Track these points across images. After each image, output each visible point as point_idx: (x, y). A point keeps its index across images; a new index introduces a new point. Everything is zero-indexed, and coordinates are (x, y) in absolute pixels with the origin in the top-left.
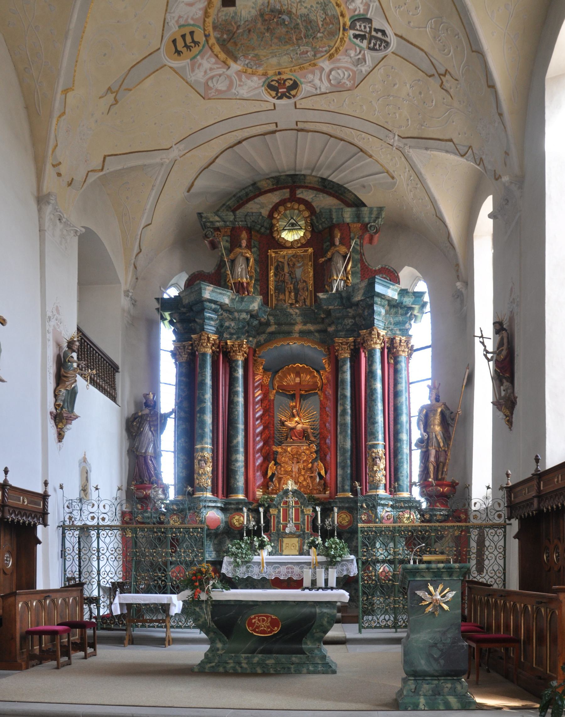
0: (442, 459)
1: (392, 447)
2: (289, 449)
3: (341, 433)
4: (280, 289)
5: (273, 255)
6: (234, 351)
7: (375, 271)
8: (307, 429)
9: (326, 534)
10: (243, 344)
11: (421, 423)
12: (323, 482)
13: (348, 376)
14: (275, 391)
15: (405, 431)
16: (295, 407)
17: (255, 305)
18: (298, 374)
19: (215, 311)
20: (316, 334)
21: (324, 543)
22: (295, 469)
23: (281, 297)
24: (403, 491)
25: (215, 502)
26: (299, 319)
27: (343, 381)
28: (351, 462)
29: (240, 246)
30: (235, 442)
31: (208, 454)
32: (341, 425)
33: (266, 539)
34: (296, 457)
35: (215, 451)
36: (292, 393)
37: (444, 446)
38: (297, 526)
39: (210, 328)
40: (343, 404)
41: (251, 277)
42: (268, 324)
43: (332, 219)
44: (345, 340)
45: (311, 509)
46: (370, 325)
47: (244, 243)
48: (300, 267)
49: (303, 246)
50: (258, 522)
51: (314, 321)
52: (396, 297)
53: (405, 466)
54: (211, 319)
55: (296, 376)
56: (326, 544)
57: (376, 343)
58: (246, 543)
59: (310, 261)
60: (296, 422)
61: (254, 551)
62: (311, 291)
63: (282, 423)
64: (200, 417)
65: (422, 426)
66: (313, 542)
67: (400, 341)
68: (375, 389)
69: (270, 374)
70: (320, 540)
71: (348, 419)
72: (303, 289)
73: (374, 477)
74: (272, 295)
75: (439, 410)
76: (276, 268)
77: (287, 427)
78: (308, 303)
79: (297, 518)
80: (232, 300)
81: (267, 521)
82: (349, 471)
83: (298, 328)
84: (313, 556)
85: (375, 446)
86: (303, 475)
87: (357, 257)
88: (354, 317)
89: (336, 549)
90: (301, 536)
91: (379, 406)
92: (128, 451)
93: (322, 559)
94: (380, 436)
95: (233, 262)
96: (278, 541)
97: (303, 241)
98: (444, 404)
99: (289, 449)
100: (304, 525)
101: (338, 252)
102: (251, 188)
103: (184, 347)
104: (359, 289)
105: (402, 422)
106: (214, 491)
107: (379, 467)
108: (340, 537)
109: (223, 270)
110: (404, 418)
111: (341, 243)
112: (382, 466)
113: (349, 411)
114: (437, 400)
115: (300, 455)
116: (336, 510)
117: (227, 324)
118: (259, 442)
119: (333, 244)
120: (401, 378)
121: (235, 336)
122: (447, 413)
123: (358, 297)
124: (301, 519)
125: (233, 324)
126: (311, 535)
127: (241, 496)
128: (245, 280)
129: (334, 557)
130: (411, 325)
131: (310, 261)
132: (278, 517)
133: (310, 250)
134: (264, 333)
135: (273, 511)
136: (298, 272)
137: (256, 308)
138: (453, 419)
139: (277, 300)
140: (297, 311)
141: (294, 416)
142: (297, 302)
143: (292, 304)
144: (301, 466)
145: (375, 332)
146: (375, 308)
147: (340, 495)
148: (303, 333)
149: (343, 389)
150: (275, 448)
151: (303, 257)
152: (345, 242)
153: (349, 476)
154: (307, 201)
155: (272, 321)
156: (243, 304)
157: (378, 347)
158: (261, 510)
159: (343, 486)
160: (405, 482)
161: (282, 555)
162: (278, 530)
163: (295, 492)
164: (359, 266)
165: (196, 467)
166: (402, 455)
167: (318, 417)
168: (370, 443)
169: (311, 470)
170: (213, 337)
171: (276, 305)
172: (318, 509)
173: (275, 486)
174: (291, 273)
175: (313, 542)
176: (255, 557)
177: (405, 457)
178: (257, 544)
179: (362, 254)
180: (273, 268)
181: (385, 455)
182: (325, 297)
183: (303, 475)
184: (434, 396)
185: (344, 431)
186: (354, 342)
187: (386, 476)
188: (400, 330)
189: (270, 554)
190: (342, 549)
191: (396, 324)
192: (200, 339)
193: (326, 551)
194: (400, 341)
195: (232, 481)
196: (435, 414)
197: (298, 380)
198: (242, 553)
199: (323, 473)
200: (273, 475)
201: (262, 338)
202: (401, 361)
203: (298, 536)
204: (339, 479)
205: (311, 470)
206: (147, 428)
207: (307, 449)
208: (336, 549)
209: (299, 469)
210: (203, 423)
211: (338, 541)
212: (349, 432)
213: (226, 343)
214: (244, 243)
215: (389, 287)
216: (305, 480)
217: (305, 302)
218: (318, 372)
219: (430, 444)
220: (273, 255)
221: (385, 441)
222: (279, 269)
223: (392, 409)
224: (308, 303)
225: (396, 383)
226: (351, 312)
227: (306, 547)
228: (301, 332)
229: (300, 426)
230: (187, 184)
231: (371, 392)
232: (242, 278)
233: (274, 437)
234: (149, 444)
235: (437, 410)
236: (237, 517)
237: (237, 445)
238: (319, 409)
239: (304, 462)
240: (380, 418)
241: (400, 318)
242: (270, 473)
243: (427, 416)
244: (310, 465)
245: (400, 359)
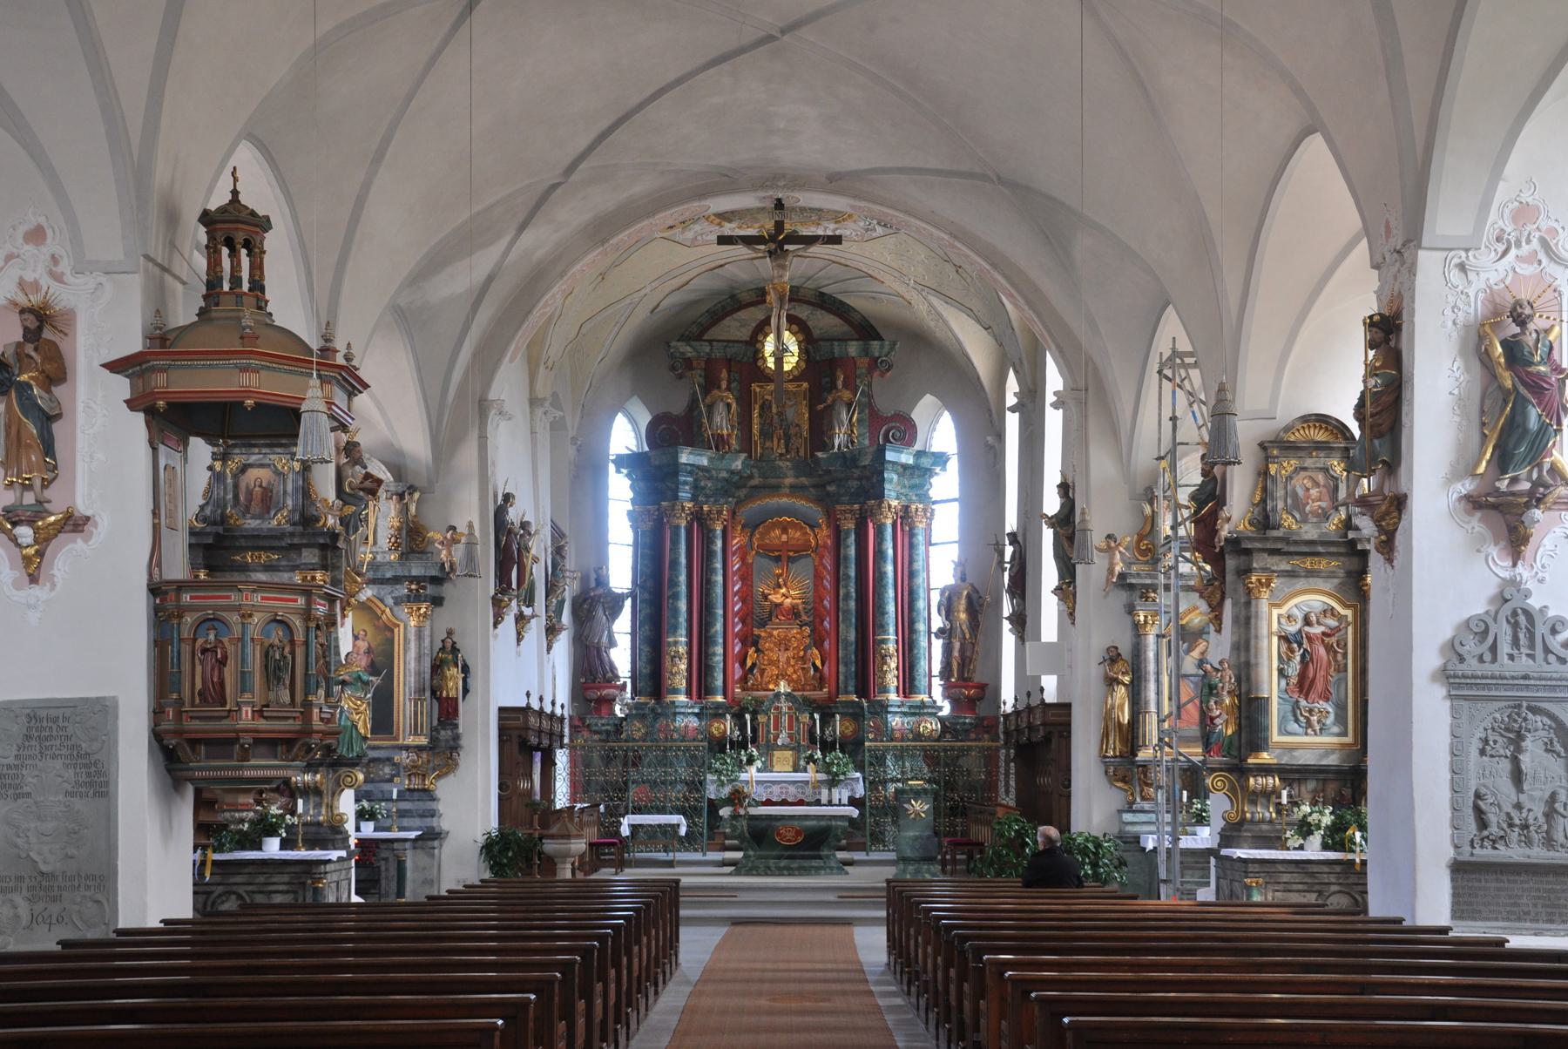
0: (968, 654)
1: (906, 636)
2: (775, 633)
3: (843, 621)
4: (766, 434)
5: (758, 390)
6: (711, 519)
7: (887, 418)
8: (797, 604)
9: (827, 747)
10: (722, 511)
11: (943, 608)
12: (818, 675)
13: (852, 552)
14: (754, 552)
15: (922, 620)
16: (781, 575)
17: (738, 464)
18: (785, 531)
19: (690, 473)
20: (811, 489)
21: (824, 757)
22: (783, 659)
23: (768, 444)
24: (920, 693)
25: (692, 707)
26: (790, 473)
27: (846, 558)
28: (856, 657)
29: (719, 387)
30: (713, 631)
31: (682, 649)
32: (844, 612)
33: (755, 753)
34: (784, 644)
35: (689, 644)
36: (777, 554)
37: (971, 638)
38: (790, 736)
39: (685, 494)
40: (846, 587)
41: (732, 427)
42: (751, 477)
43: (833, 353)
44: (848, 507)
45: (808, 716)
46: (880, 496)
47: (724, 385)
48: (792, 406)
49: (795, 379)
50: (743, 728)
51: (810, 475)
52: (911, 461)
53: (922, 663)
54: (686, 483)
55: (783, 533)
56: (827, 760)
57: (886, 517)
58: (732, 758)
59: (805, 399)
60: (783, 595)
61: (740, 766)
62: (806, 438)
63: (765, 597)
64: (672, 604)
65: (944, 613)
66: (811, 756)
67: (917, 509)
68: (885, 573)
69: (748, 530)
70: (819, 755)
71: (852, 604)
72: (796, 435)
73: (883, 678)
74: (756, 442)
75: (965, 593)
76: (762, 407)
77: (772, 602)
78: (802, 453)
79: (790, 728)
80: (711, 459)
81: (754, 730)
82: (853, 669)
83: (788, 481)
84: (811, 774)
85: (884, 641)
86: (793, 666)
87: (865, 400)
88: (860, 479)
89: (838, 765)
90: (796, 748)
91: (891, 593)
92: (574, 639)
93: (822, 776)
94: (892, 629)
95: (710, 408)
96: (767, 754)
97: (796, 373)
98: (972, 585)
99: (775, 633)
100: (799, 735)
101: (840, 398)
102: (729, 301)
103: (649, 511)
104: (866, 454)
105: (919, 609)
106: (689, 693)
107: (889, 667)
108: (843, 751)
109: (695, 413)
110: (921, 604)
111: (845, 386)
112: (893, 665)
113: (854, 594)
114: (963, 579)
115: (789, 641)
116: (838, 717)
117: (702, 484)
118: (738, 623)
119: (834, 386)
120: (918, 555)
121: (712, 499)
122: (975, 596)
123: (866, 461)
124: (795, 728)
125: (709, 485)
126: (808, 749)
127: (720, 699)
128: (725, 432)
129: (836, 774)
130: (931, 484)
131: (805, 399)
132: (768, 725)
133: (805, 385)
134: (744, 486)
135: (761, 718)
136: (790, 413)
137: (740, 467)
138: (982, 605)
139: (762, 448)
140: (788, 464)
141: (780, 587)
142: (788, 452)
143: (781, 455)
144: (790, 654)
145: (885, 505)
146: (886, 475)
147: (842, 698)
148: (796, 490)
149: (846, 567)
150: (756, 632)
151: (794, 394)
152: (850, 385)
153: (853, 674)
154: (801, 319)
155: (756, 475)
156: (724, 462)
157: (889, 522)
158: (748, 716)
159: (846, 687)
160: (922, 682)
161: (772, 771)
162: (768, 741)
163: (788, 695)
164: (867, 411)
165: (668, 663)
166: (919, 649)
167: (812, 586)
168: (879, 637)
169: (803, 659)
170: (688, 505)
171: (762, 455)
172: (816, 716)
173: (756, 680)
174: (780, 414)
175: (811, 756)
176: (742, 775)
177: (922, 652)
178: (745, 759)
179: (870, 397)
180: (757, 407)
181: (897, 651)
182: (825, 456)
183: (793, 666)
184: (959, 575)
185: (846, 619)
186: (861, 509)
187: (898, 677)
188: (916, 495)
189: (759, 770)
190: (846, 765)
191: (912, 487)
192: (673, 509)
193: (826, 768)
194: (917, 509)
195: (709, 680)
196: (959, 598)
197: (784, 537)
198: (727, 770)
199: (818, 663)
200: (754, 665)
201: (742, 493)
202: (917, 534)
203: (792, 749)
204: (841, 678)
205: (803, 659)
206: (600, 612)
207: (798, 633)
208: (838, 765)
209: (788, 659)
210: (676, 611)
211: (841, 755)
212: (854, 620)
213: (702, 508)
214: (724, 385)
215: (902, 452)
216: (795, 672)
217: (798, 452)
218: (812, 527)
219: (953, 635)
220: (758, 390)
221: (897, 635)
222: (765, 407)
223: (906, 593)
224: (802, 453)
225: (911, 562)
226: (857, 472)
227: (802, 763)
228: (792, 487)
229: (788, 601)
230: (651, 307)
231: (880, 576)
232: (722, 430)
233: (752, 613)
234: (603, 632)
235: (962, 594)
236: (716, 725)
237: (714, 636)
238: (812, 576)
239: (794, 648)
240: (891, 608)
241: (917, 481)
242: (749, 663)
243: (949, 599)
244: (802, 653)
245: (916, 531)
